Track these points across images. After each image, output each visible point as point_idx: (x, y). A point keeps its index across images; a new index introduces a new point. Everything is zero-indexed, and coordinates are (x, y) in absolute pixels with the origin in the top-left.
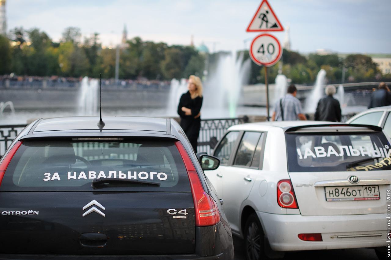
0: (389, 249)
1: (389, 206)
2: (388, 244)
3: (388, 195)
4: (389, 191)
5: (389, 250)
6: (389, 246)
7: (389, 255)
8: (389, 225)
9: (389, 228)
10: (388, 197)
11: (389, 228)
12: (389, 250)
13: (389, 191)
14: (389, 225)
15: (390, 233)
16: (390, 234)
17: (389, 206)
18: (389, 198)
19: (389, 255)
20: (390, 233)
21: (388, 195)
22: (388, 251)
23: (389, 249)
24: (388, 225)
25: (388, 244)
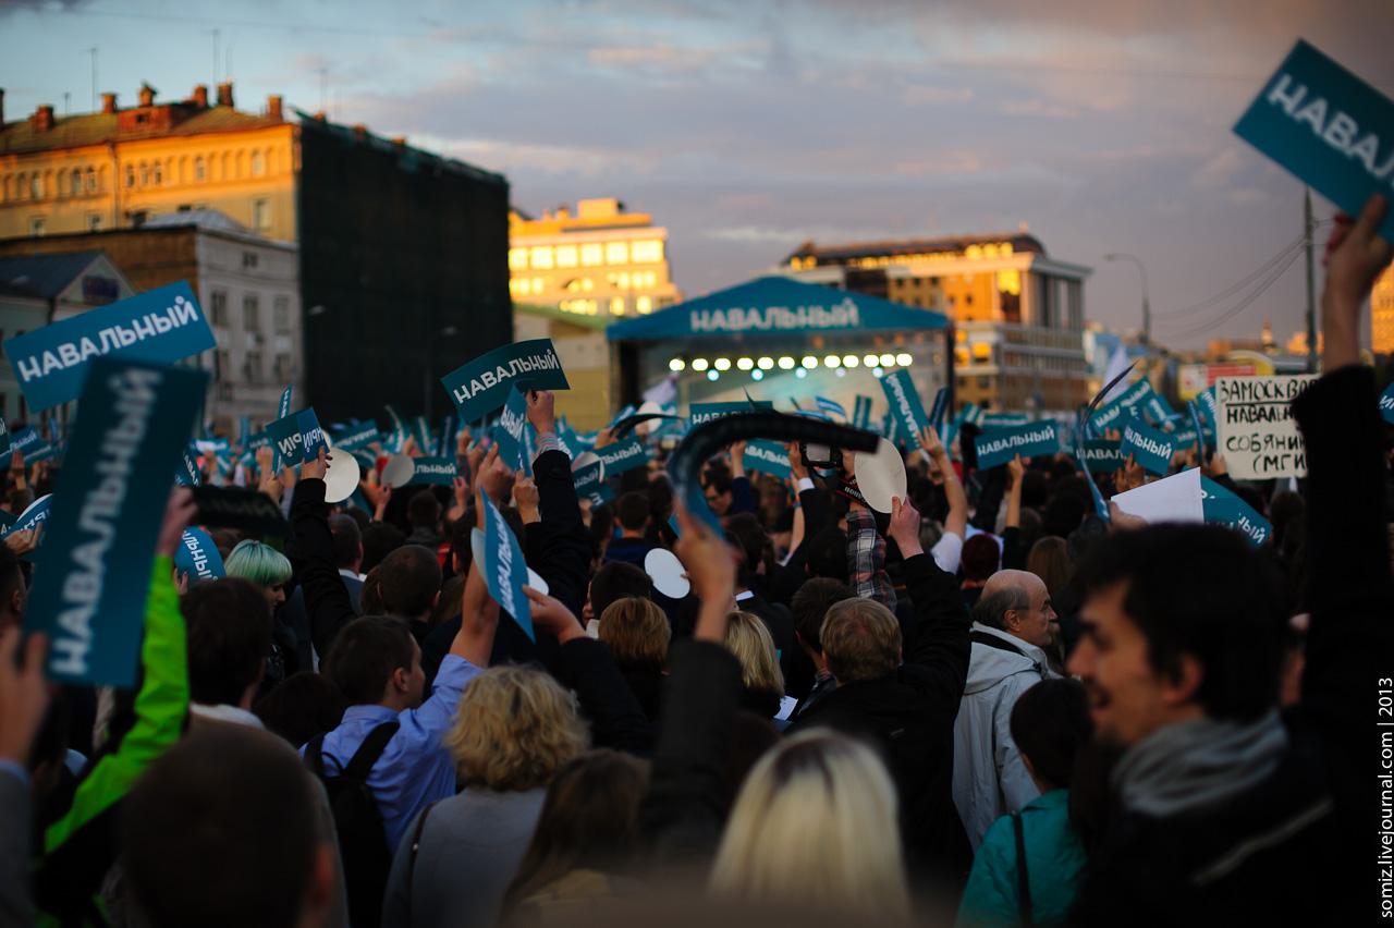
0: (1386, 887)
1: (1386, 737)
2: (1384, 871)
3: (1384, 695)
4: (1388, 682)
5: (1386, 893)
6: (1386, 877)
7: (1386, 911)
8: (1387, 801)
9: (1388, 813)
10: (1388, 702)
11: (1388, 813)
12: (1386, 893)
13: (1388, 682)
14: (1387, 801)
17: (1386, 737)
18: (1388, 708)
19: (1386, 911)
21: (1384, 695)
22: (1384, 896)
23: (1386, 887)
24: (1385, 804)
25: (1384, 871)
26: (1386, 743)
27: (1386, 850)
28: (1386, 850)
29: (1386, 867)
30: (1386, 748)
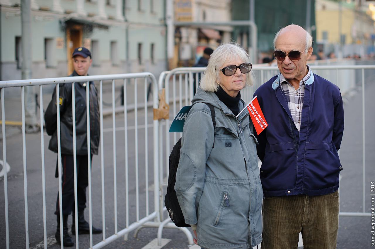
0: (373, 238)
1: (373, 198)
2: (372, 234)
3: (372, 186)
4: (373, 183)
5: (373, 240)
6: (373, 235)
9: (373, 218)
10: (373, 188)
11: (373, 218)
12: (373, 240)
13: (373, 183)
15: (374, 223)
16: (374, 224)
17: (373, 198)
18: (373, 190)
19: (373, 245)
20: (374, 223)
21: (372, 186)
22: (372, 240)
23: (373, 238)
25: (372, 234)
26: (373, 199)
27: (373, 228)
28: (373, 228)
29: (373, 233)
30: (373, 201)
